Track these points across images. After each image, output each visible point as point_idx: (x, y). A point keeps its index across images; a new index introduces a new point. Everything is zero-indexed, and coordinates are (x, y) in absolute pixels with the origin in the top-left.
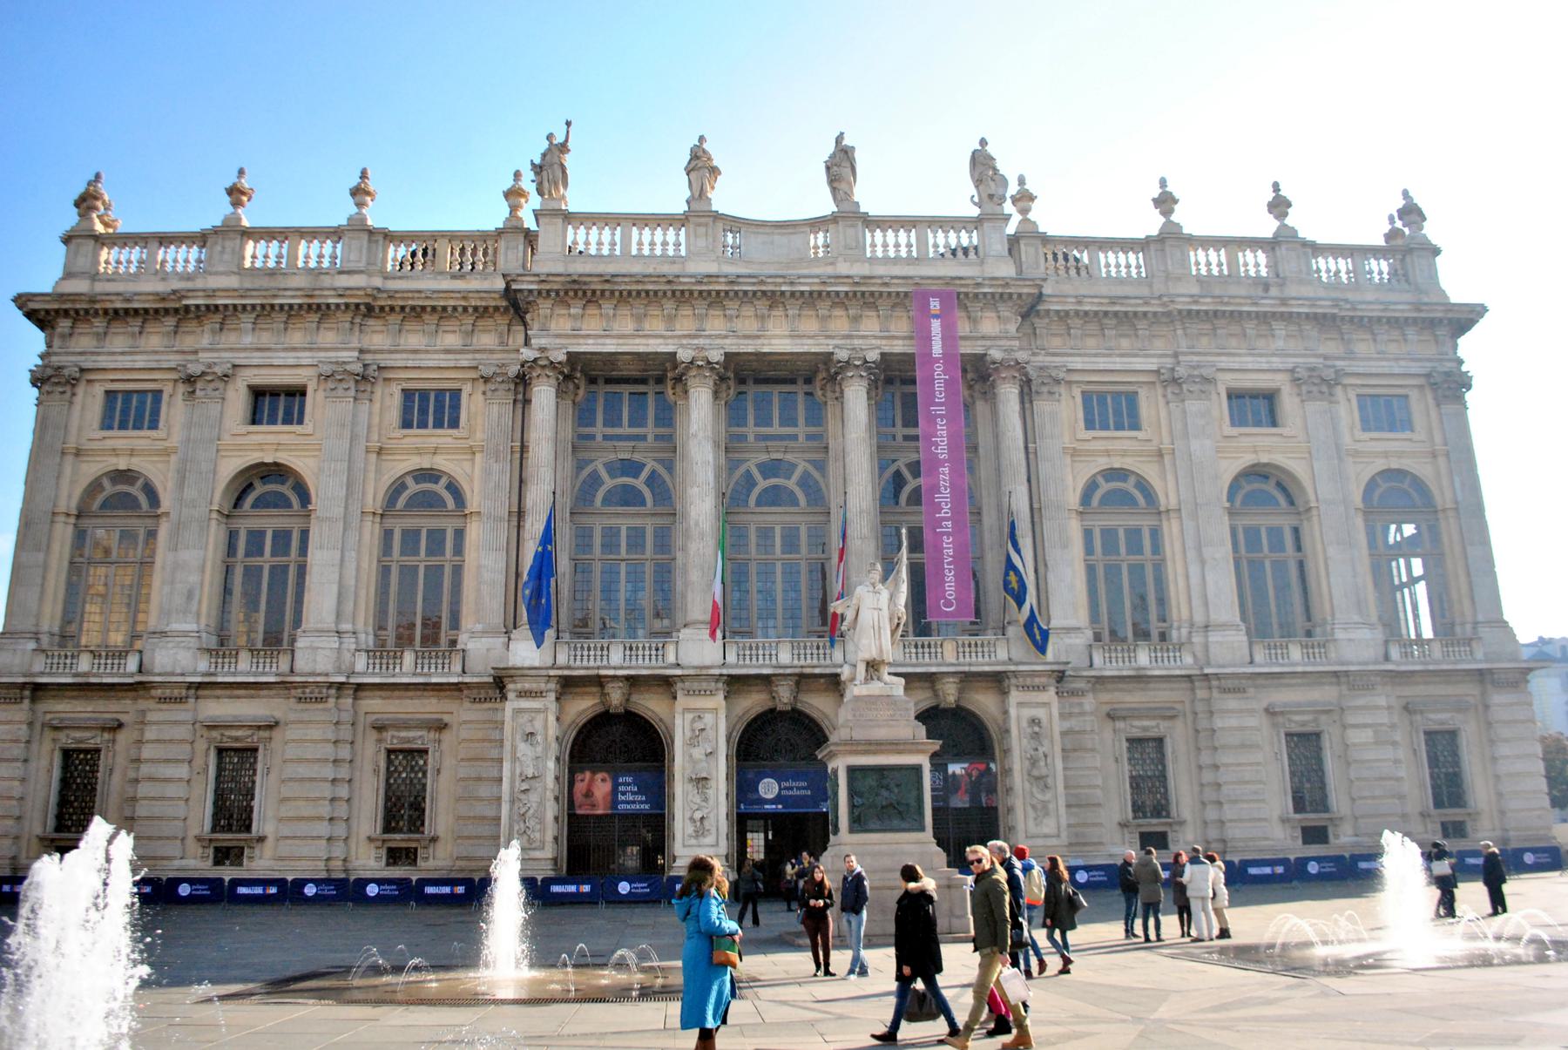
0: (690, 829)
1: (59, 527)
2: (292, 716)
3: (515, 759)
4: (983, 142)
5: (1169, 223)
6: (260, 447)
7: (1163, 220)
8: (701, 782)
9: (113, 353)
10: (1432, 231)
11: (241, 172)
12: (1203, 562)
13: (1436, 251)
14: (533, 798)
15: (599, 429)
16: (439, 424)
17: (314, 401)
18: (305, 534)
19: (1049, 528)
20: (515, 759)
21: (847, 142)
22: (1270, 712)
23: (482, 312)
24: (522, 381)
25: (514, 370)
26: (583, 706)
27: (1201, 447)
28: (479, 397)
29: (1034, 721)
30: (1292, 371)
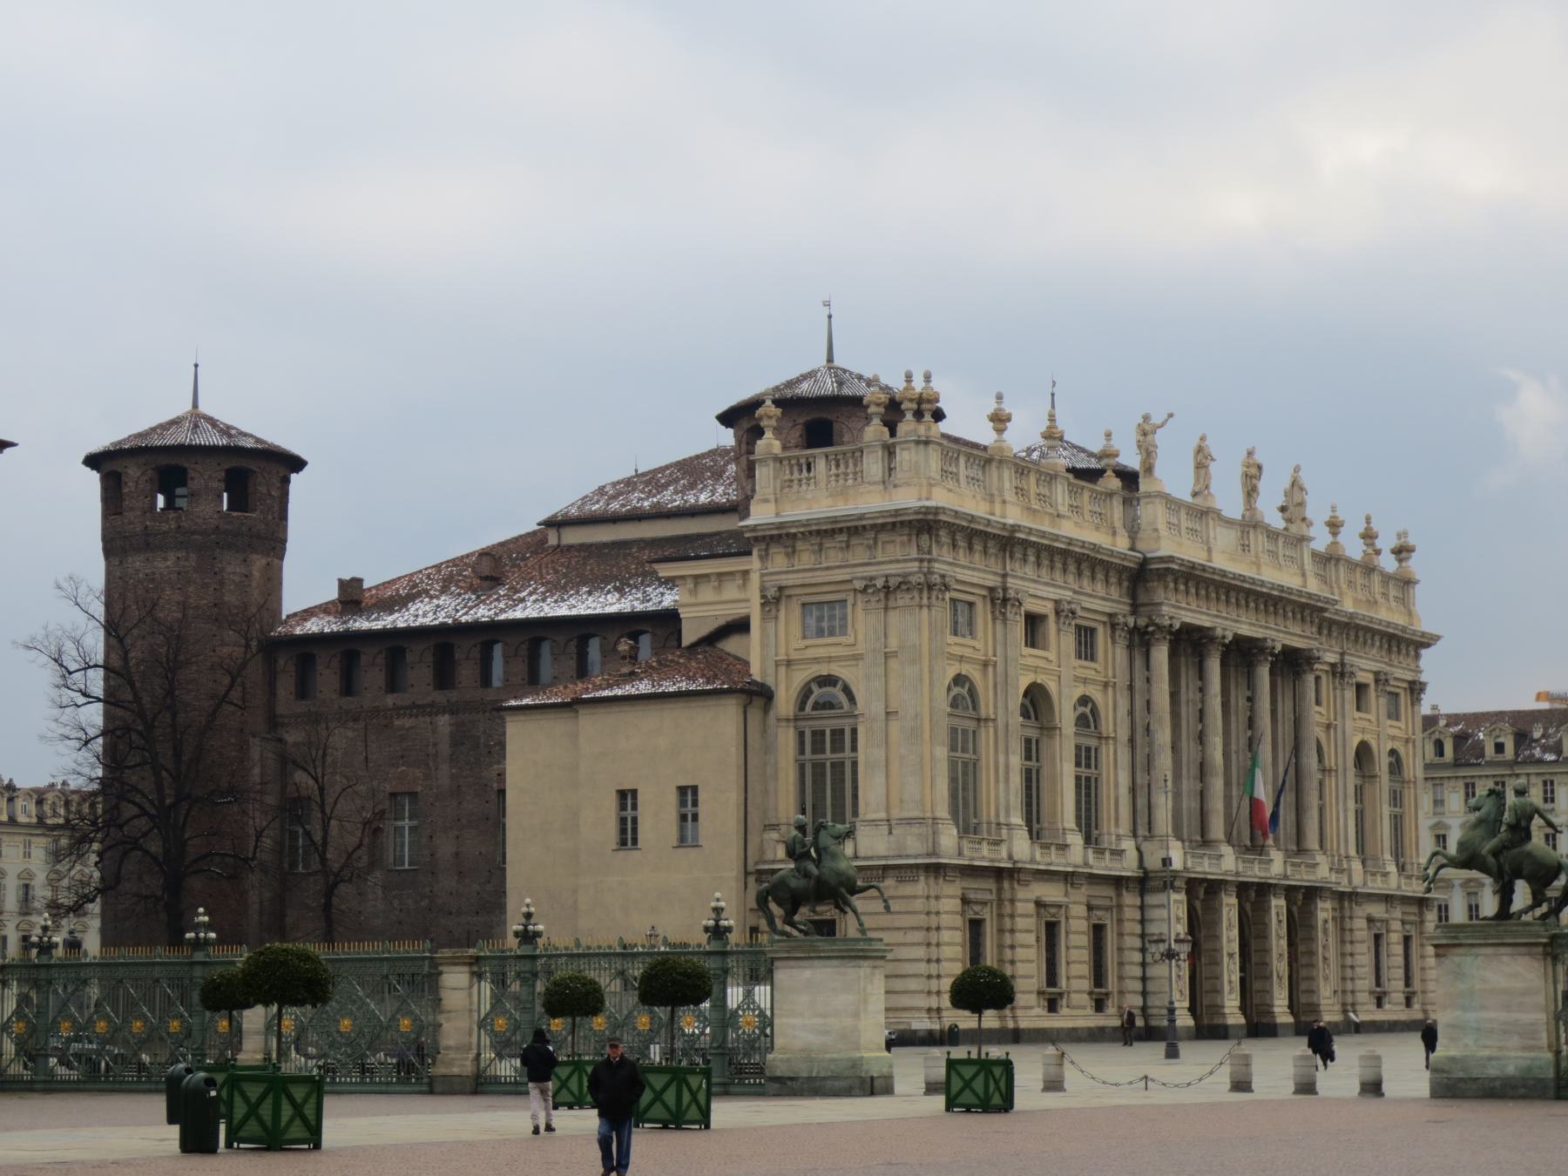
2: (1072, 898)
4: (1297, 469)
5: (1335, 543)
6: (1036, 669)
7: (1330, 539)
8: (1231, 955)
9: (964, 567)
10: (1415, 564)
11: (999, 397)
12: (1345, 811)
13: (1416, 582)
21: (1259, 457)
22: (1370, 920)
23: (1121, 570)
27: (1349, 724)
30: (1377, 674)
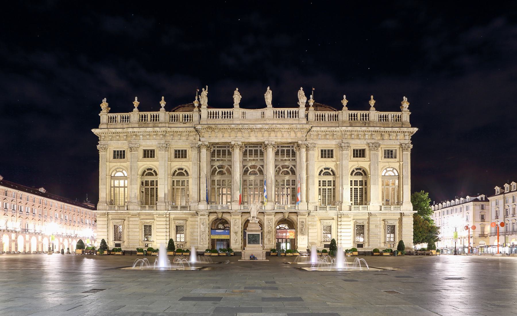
0: (234, 242)
1: (108, 179)
3: (200, 228)
8: (236, 233)
14: (204, 235)
15: (216, 158)
16: (182, 157)
17: (157, 153)
18: (157, 181)
19: (310, 181)
20: (200, 228)
24: (199, 147)
25: (197, 146)
26: (213, 217)
28: (190, 151)
29: (302, 222)
